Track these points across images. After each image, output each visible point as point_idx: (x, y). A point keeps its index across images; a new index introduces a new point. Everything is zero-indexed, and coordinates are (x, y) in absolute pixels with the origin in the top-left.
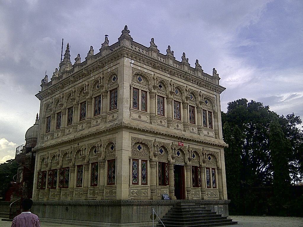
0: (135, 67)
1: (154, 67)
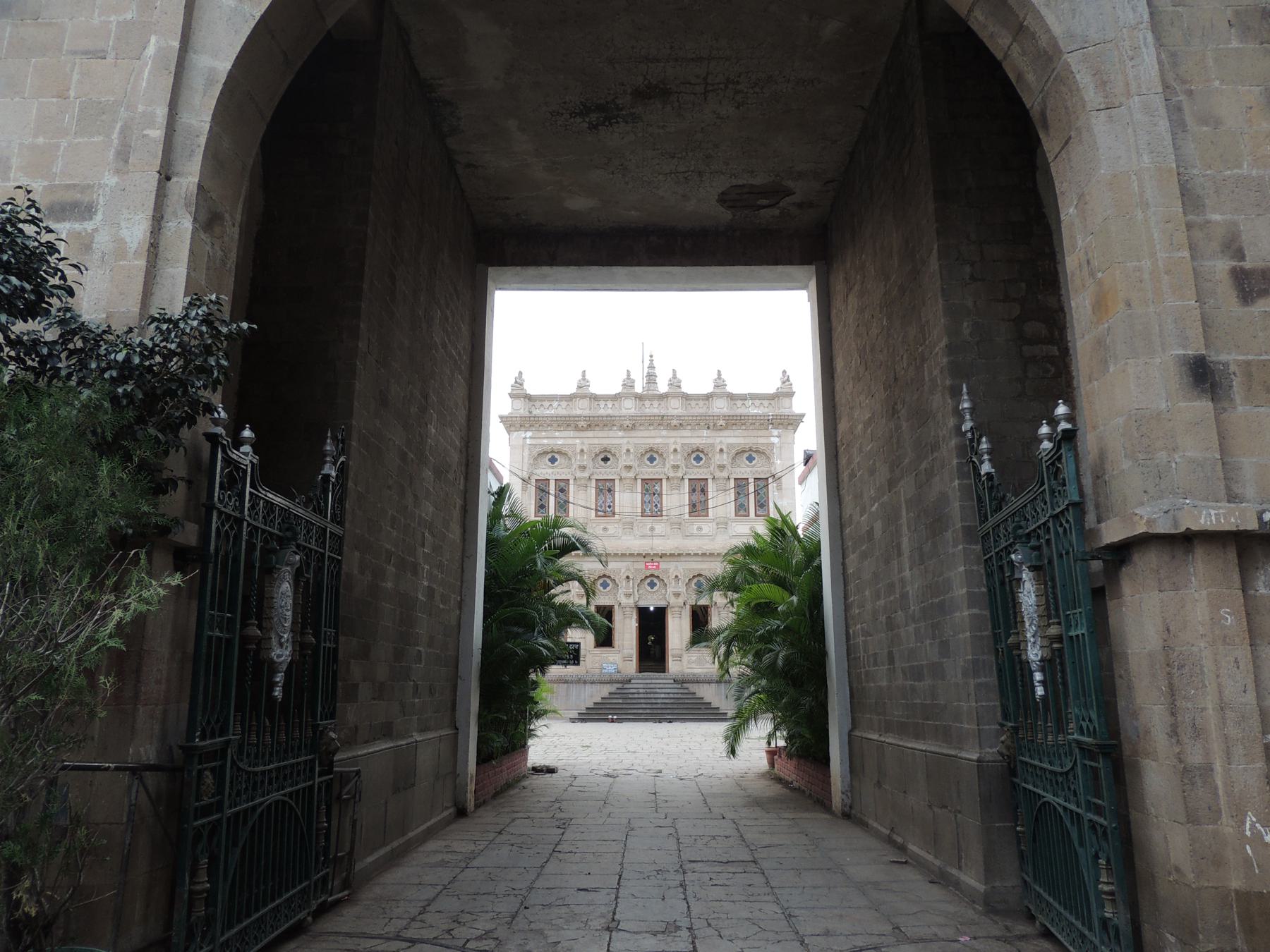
0: (534, 442)
1: (576, 428)
